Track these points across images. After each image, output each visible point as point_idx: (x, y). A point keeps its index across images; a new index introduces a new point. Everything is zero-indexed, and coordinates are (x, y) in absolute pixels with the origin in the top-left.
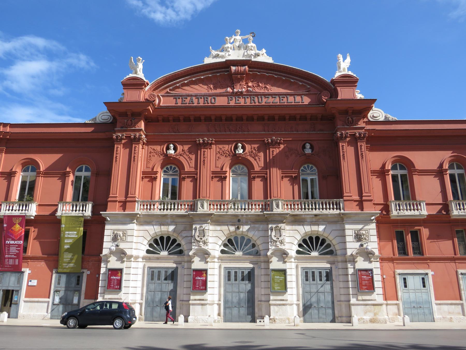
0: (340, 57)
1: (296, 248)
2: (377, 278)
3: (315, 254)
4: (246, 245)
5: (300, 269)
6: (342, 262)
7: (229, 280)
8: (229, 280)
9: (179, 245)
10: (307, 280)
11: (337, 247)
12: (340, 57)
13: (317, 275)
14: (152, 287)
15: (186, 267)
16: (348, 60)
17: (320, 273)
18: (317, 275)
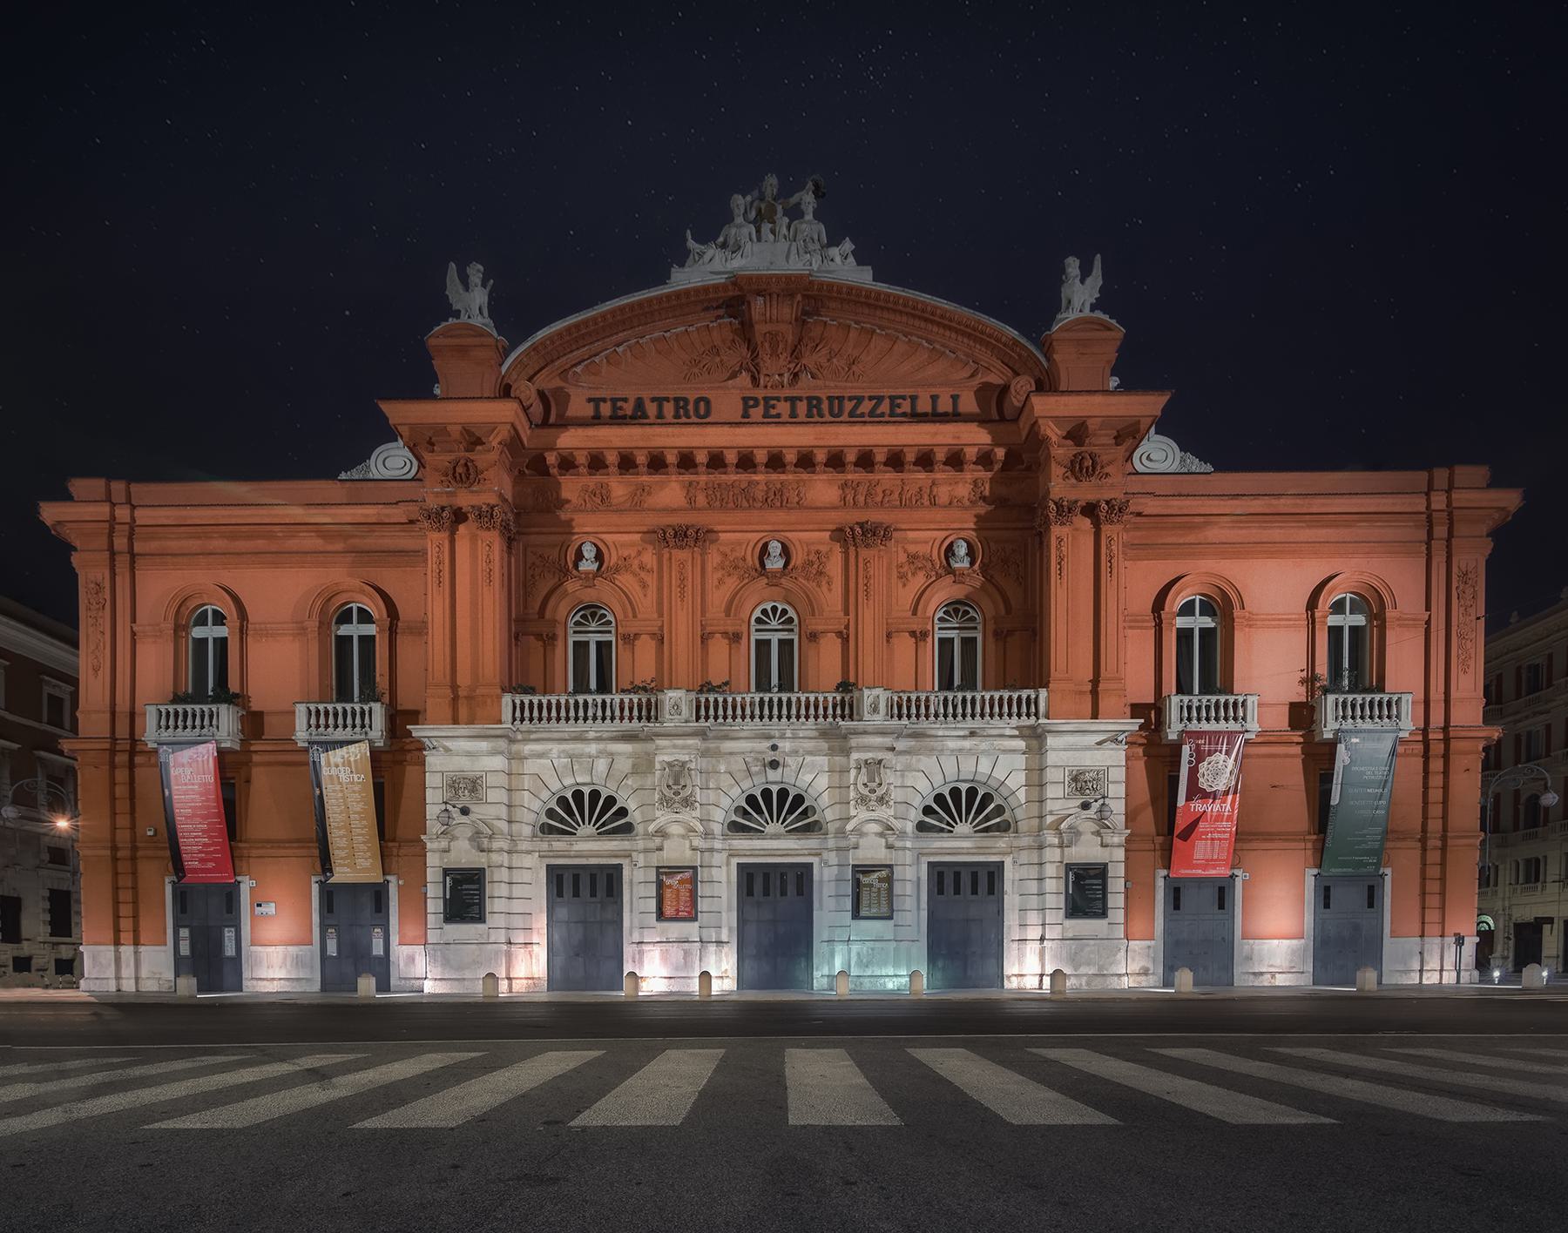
0: (1073, 265)
1: (916, 815)
2: (1116, 885)
3: (963, 828)
4: (790, 812)
5: (924, 867)
6: (1030, 848)
7: (750, 893)
8: (750, 893)
9: (623, 812)
10: (941, 892)
11: (1019, 814)
12: (1073, 265)
13: (966, 880)
14: (562, 913)
15: (641, 864)
16: (1096, 279)
17: (975, 876)
18: (966, 880)
